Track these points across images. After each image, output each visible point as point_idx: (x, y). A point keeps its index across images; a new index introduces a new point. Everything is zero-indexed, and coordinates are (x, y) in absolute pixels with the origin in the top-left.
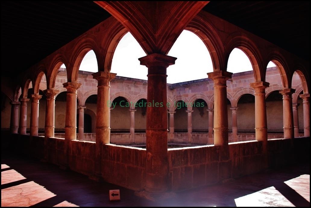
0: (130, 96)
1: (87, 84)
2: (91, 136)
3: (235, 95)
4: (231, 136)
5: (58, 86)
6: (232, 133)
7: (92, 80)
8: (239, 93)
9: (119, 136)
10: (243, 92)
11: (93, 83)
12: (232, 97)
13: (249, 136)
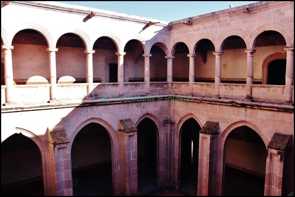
0: (283, 26)
1: (220, 26)
2: (228, 87)
5: (194, 35)
7: (225, 20)
9: (264, 88)
11: (228, 22)
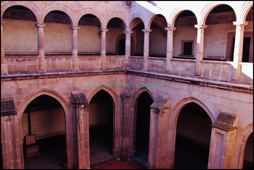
3: (44, 8)
4: (37, 59)
6: (38, 56)
8: (50, 6)
10: (55, 7)
12: (40, 11)
13: (61, 59)
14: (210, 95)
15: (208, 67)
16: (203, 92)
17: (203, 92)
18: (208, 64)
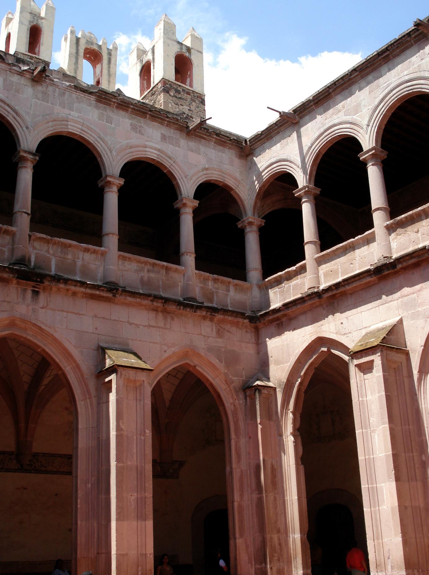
14: (68, 312)
15: (48, 251)
16: (47, 305)
17: (47, 305)
18: (46, 245)
